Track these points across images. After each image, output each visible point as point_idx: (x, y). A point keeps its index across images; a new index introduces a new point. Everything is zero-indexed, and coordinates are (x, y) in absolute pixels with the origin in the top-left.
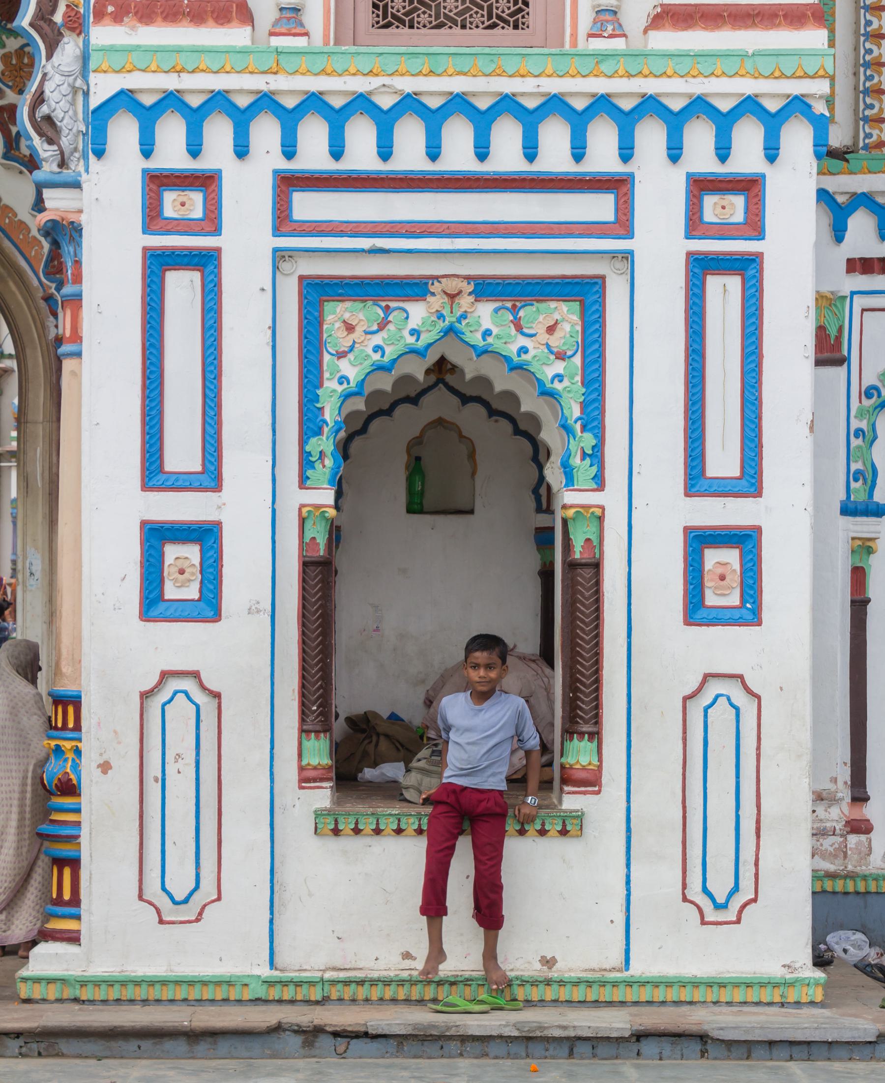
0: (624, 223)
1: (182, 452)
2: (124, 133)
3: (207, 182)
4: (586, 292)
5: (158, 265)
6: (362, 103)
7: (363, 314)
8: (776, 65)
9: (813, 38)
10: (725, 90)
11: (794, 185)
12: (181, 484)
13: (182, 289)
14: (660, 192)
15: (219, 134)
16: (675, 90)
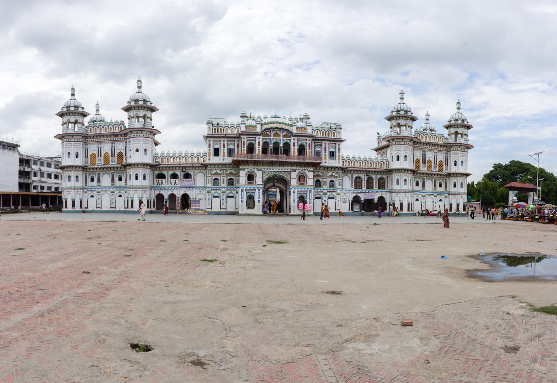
11: (312, 190)
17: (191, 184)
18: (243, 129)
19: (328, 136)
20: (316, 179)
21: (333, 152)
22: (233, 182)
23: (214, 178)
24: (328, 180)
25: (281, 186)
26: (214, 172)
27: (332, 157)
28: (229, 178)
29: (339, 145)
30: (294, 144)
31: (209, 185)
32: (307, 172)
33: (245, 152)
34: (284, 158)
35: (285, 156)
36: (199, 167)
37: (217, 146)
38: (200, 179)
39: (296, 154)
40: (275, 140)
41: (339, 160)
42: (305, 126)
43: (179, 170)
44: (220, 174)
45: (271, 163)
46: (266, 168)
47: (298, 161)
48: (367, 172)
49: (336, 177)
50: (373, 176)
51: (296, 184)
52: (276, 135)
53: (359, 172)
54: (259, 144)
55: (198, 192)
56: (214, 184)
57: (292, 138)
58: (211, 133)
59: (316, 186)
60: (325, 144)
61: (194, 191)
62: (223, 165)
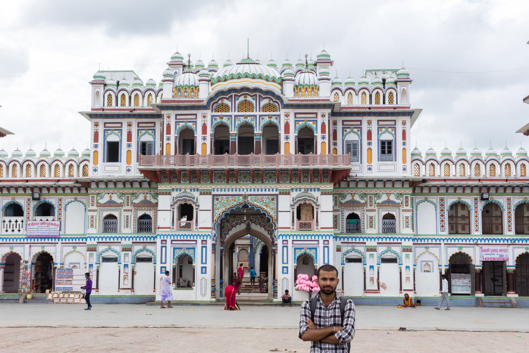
0: (318, 244)
1: (285, 261)
2: (281, 237)
3: (287, 241)
4: (316, 249)
5: (283, 247)
6: (299, 235)
7: (299, 250)
8: (330, 232)
9: (333, 230)
10: (326, 234)
11: (331, 240)
12: (285, 263)
13: (285, 249)
14: (321, 241)
15: (288, 237)
16: (322, 234)
17: (53, 230)
18: (168, 94)
19: (377, 102)
20: (347, 213)
21: (390, 143)
22: (150, 224)
23: (105, 214)
24: (378, 215)
25: (262, 230)
26: (106, 199)
27: (387, 156)
28: (140, 213)
29: (404, 123)
30: (287, 126)
31: (93, 231)
32: (316, 194)
33: (172, 153)
34: (259, 161)
35: (263, 156)
36: (72, 189)
37: (113, 138)
38: (75, 217)
39: (292, 150)
40: (242, 119)
41: (404, 161)
42: (317, 82)
43: (25, 194)
44: (121, 205)
45: (231, 176)
46: (221, 188)
47: (295, 166)
48: (483, 189)
49: (398, 205)
50: (501, 200)
51: (288, 224)
52: (246, 106)
53: (460, 191)
54: (204, 131)
55: (71, 249)
56: (106, 230)
57: (283, 112)
58: (100, 106)
59: (349, 231)
60: (369, 123)
61: (59, 246)
62: (124, 182)
